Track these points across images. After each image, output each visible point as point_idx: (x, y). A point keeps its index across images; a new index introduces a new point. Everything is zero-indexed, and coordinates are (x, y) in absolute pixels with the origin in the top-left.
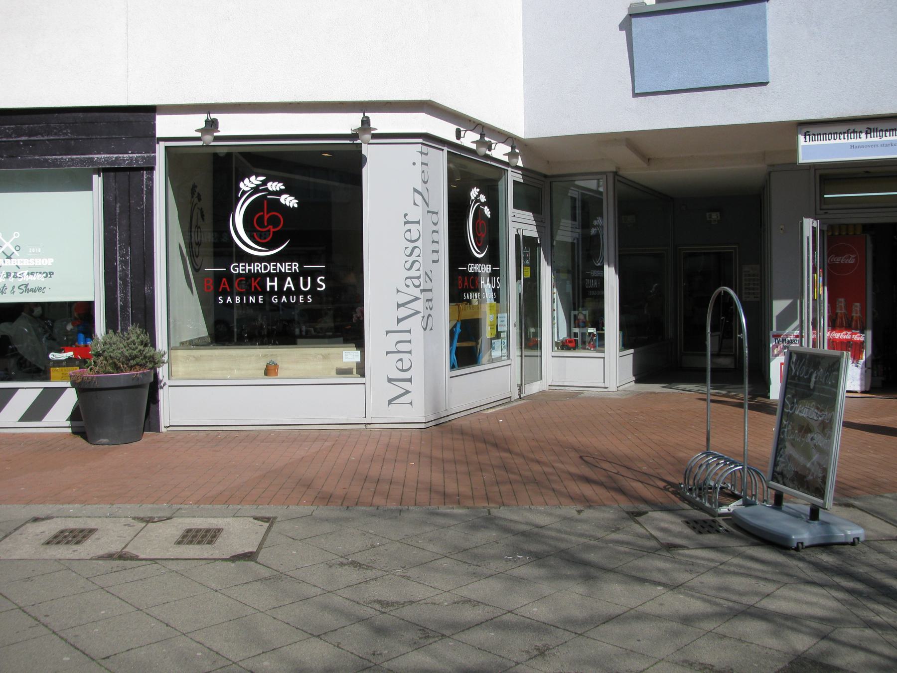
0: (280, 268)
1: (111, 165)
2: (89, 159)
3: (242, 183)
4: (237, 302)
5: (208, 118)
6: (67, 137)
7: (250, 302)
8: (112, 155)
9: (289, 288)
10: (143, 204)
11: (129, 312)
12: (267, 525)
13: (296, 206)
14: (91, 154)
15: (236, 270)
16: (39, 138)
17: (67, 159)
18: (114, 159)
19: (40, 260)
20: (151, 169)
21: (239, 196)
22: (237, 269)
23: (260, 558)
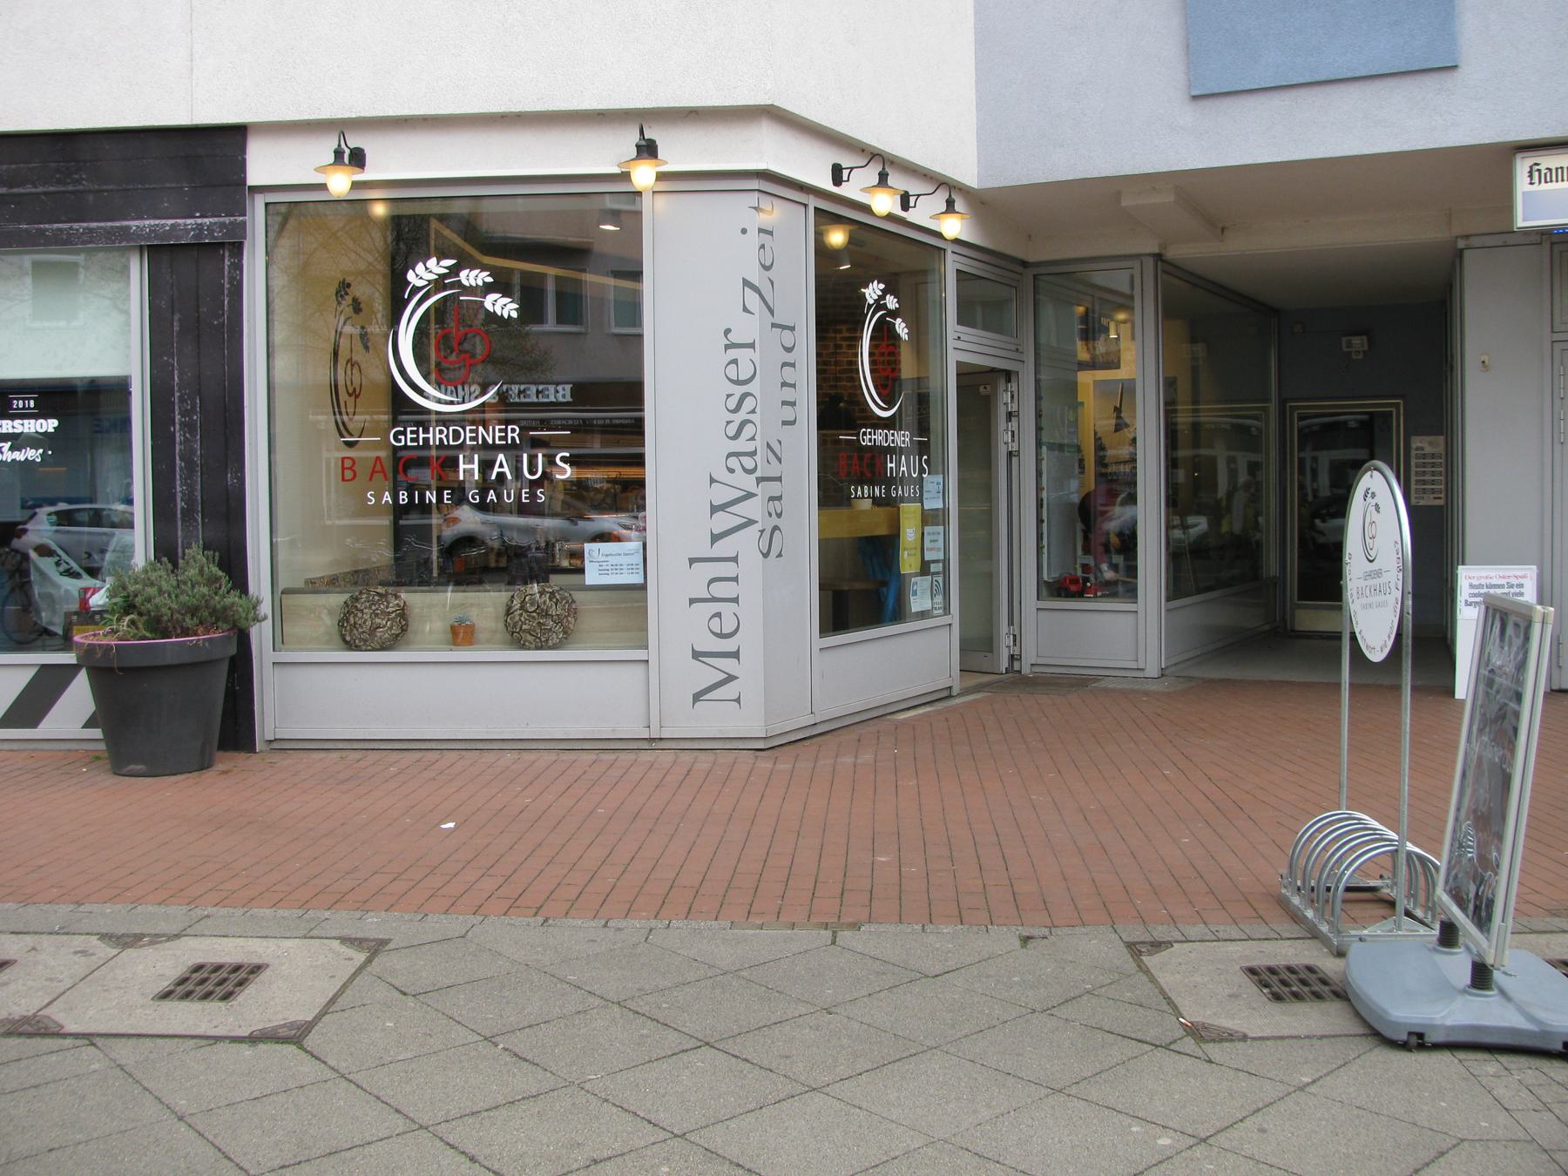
0: (483, 436)
1: (162, 240)
2: (121, 228)
3: (411, 271)
4: (401, 502)
5: (339, 145)
6: (81, 187)
7: (427, 502)
8: (163, 221)
9: (501, 476)
10: (223, 315)
11: (196, 521)
12: (361, 957)
13: (514, 315)
14: (125, 219)
15: (400, 441)
16: (29, 189)
17: (81, 230)
18: (168, 228)
19: (33, 421)
20: (237, 248)
21: (406, 297)
22: (403, 437)
23: (309, 1042)
